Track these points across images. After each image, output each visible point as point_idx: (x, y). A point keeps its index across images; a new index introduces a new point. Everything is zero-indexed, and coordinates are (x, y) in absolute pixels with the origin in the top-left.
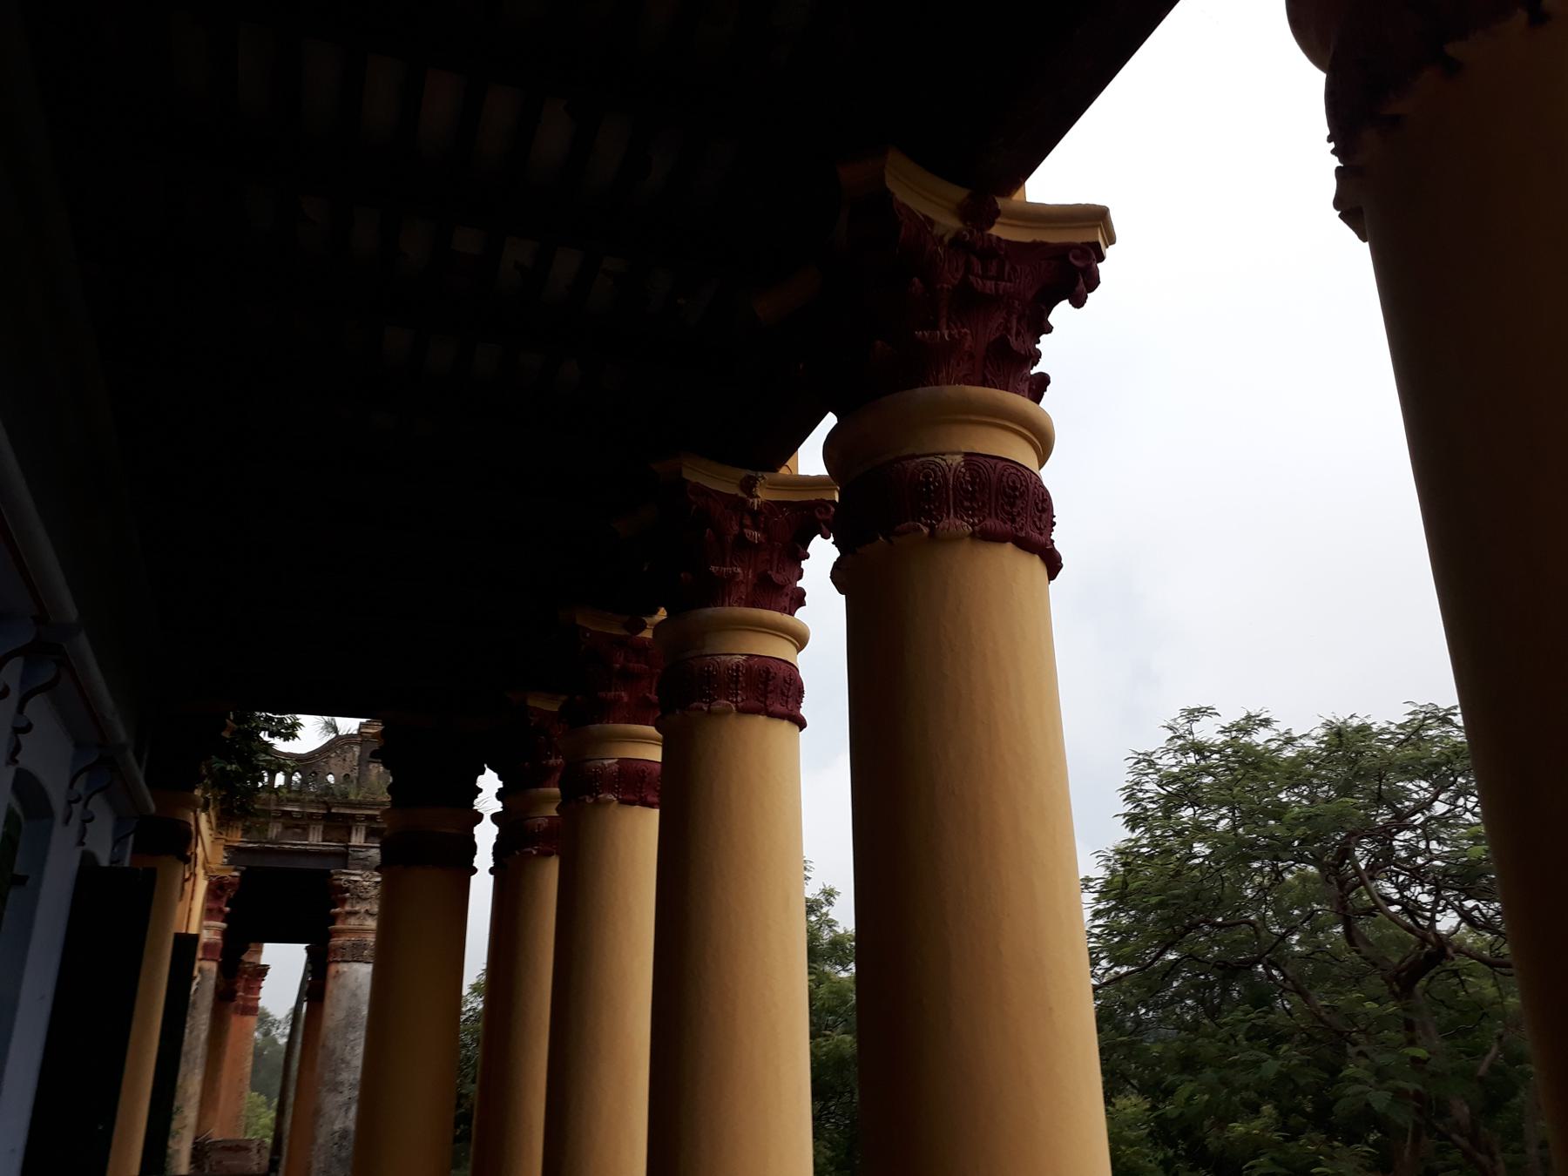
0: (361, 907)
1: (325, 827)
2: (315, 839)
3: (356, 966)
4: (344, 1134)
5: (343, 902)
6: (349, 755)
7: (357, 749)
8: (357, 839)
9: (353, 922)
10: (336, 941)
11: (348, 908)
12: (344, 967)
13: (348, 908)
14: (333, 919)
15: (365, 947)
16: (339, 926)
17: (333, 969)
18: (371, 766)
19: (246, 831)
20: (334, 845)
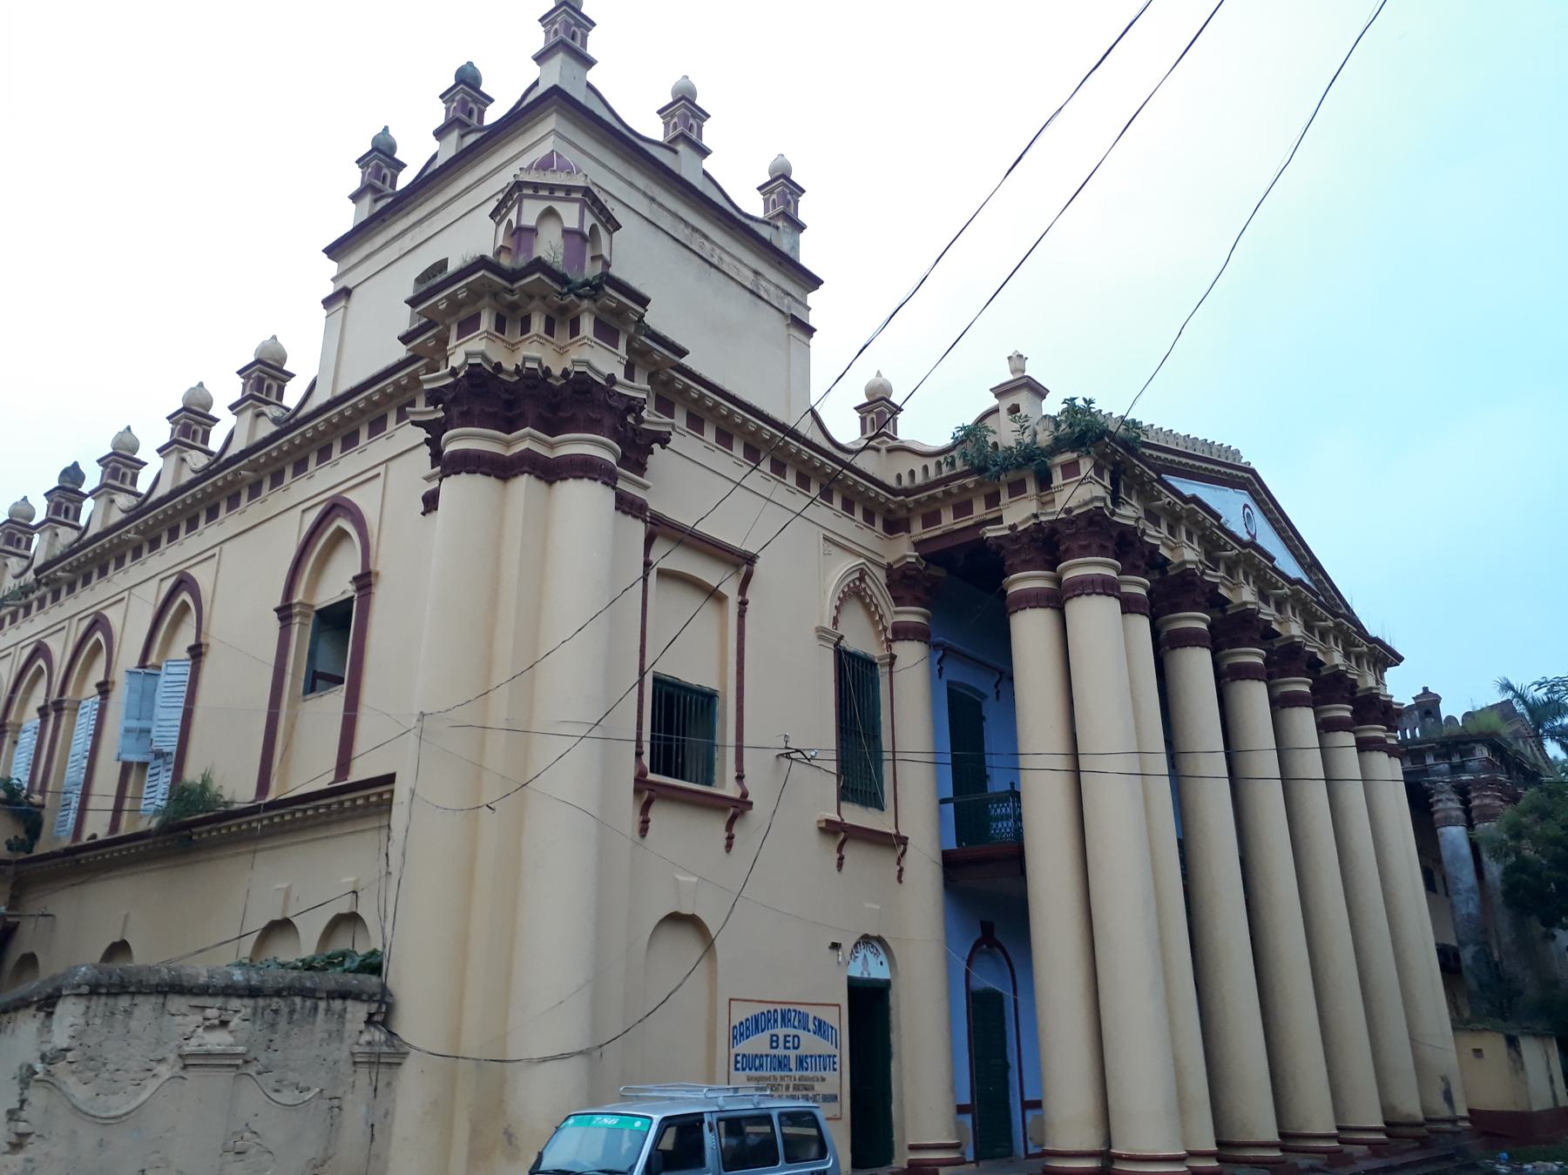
0: (1443, 797)
3: (1449, 828)
4: (1469, 915)
5: (1431, 796)
6: (1413, 717)
7: (1416, 713)
8: (1430, 761)
9: (1440, 805)
10: (1436, 816)
11: (1435, 798)
12: (1443, 830)
13: (1435, 798)
14: (1432, 805)
15: (1451, 817)
16: (1435, 808)
17: (1439, 831)
18: (1427, 719)
20: (1419, 766)
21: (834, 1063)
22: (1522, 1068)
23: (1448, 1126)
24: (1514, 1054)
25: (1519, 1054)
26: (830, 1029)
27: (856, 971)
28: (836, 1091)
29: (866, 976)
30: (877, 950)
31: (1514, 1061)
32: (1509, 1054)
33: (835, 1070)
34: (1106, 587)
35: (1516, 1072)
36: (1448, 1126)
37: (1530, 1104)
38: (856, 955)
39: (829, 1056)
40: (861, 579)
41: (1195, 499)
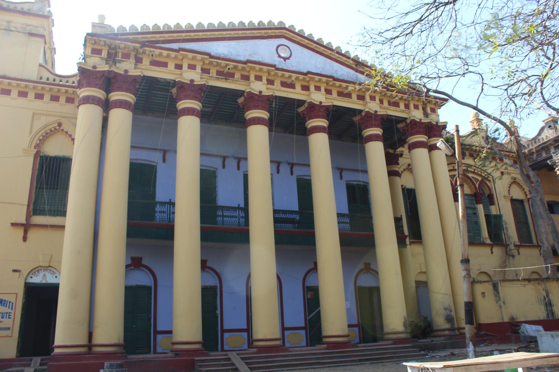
1: (545, 151)
2: (544, 155)
19: (529, 161)
21: (9, 315)
22: (499, 299)
23: (447, 332)
24: (495, 292)
25: (498, 293)
26: (8, 303)
27: (37, 279)
28: (11, 326)
29: (44, 282)
30: (53, 272)
31: (496, 296)
32: (495, 294)
33: (9, 318)
34: (87, 100)
35: (497, 302)
36: (447, 332)
37: (503, 319)
38: (38, 274)
39: (7, 313)
40: (60, 125)
41: (181, 49)
